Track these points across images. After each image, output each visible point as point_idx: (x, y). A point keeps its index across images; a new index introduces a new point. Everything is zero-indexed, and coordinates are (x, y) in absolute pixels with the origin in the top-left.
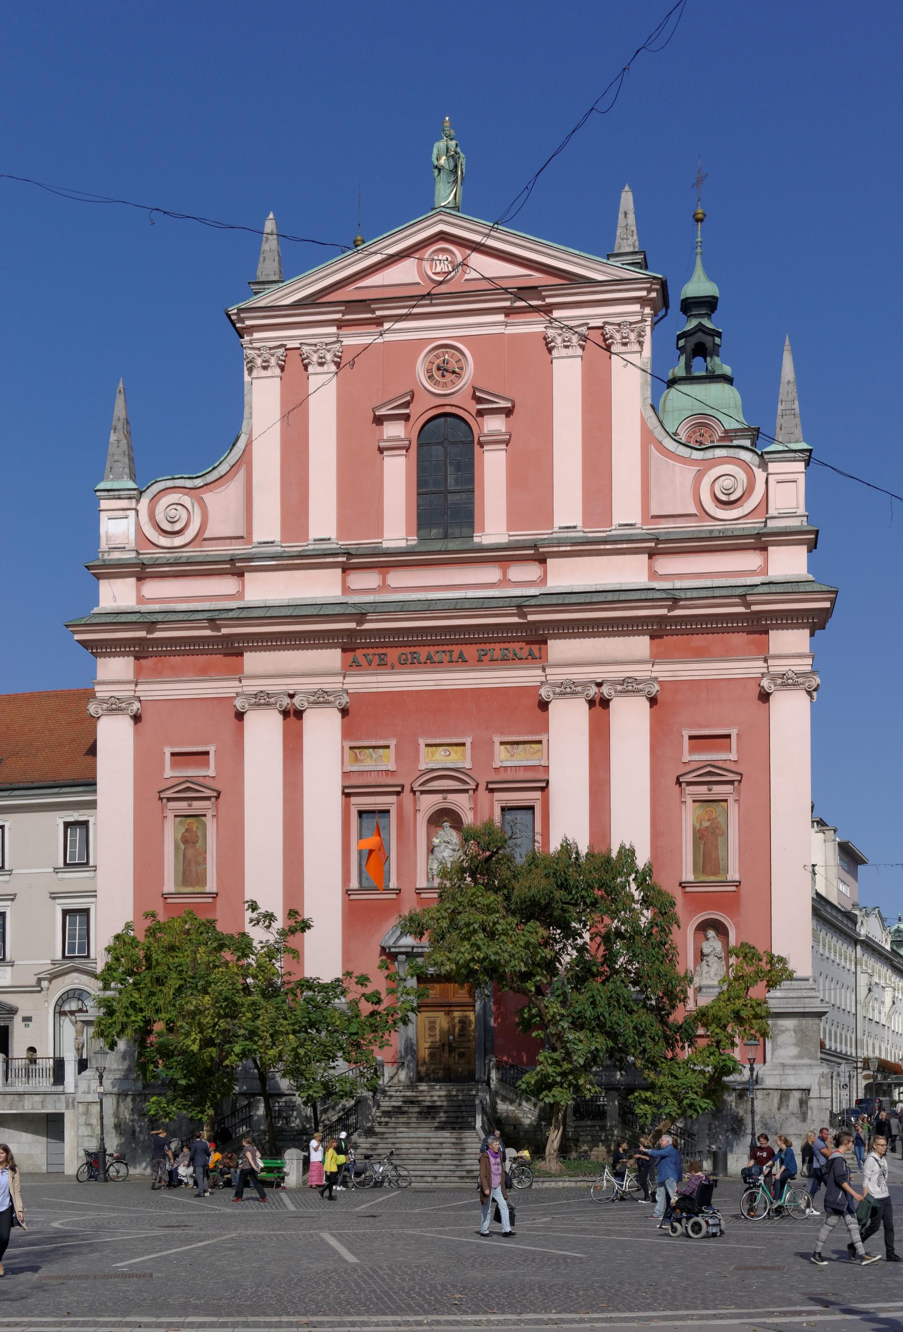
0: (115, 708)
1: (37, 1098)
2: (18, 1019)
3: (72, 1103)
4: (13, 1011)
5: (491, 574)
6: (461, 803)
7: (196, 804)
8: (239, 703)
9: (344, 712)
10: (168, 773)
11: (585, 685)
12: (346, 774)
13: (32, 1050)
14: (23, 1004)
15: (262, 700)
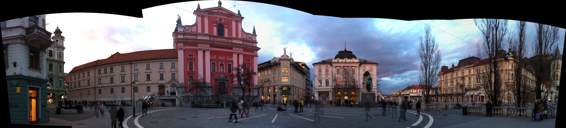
0: (181, 49)
1: (172, 97)
2: (166, 88)
3: (177, 97)
4: (165, 86)
5: (227, 40)
6: (224, 63)
7: (192, 61)
8: (198, 49)
9: (210, 52)
10: (188, 57)
11: (237, 52)
12: (210, 59)
13: (167, 91)
14: (166, 85)
15: (201, 49)
